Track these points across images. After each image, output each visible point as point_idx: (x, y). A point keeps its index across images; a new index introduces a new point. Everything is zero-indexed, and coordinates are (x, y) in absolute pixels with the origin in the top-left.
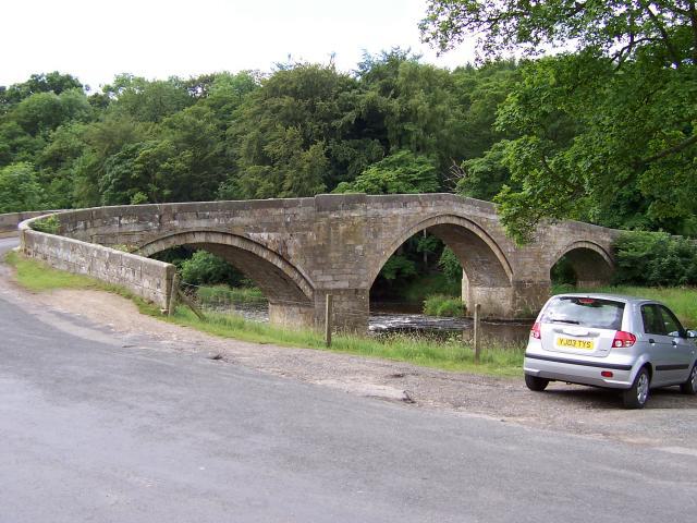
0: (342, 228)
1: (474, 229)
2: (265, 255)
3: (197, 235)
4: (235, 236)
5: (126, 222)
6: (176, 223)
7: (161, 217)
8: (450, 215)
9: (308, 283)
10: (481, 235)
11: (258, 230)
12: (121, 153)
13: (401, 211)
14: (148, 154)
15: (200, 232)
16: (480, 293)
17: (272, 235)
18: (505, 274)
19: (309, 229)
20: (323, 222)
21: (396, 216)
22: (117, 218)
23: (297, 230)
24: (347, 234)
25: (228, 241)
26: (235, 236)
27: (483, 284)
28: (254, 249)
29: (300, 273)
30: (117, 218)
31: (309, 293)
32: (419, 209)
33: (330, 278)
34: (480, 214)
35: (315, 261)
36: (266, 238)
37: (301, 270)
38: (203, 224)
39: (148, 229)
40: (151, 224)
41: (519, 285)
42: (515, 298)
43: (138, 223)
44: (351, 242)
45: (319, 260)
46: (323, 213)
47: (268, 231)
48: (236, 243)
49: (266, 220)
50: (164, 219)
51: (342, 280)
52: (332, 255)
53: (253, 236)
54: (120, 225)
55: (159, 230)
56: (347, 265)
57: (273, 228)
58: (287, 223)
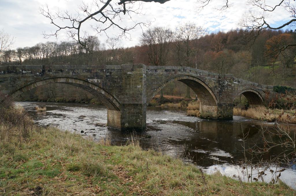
1: (200, 82)
4: (81, 80)
5: (25, 72)
9: (117, 101)
10: (203, 84)
18: (214, 101)
25: (78, 82)
26: (81, 80)
27: (206, 104)
30: (21, 70)
39: (37, 75)
40: (38, 73)
42: (218, 110)
43: (31, 73)
47: (97, 78)
48: (81, 83)
53: (90, 80)
58: (107, 76)
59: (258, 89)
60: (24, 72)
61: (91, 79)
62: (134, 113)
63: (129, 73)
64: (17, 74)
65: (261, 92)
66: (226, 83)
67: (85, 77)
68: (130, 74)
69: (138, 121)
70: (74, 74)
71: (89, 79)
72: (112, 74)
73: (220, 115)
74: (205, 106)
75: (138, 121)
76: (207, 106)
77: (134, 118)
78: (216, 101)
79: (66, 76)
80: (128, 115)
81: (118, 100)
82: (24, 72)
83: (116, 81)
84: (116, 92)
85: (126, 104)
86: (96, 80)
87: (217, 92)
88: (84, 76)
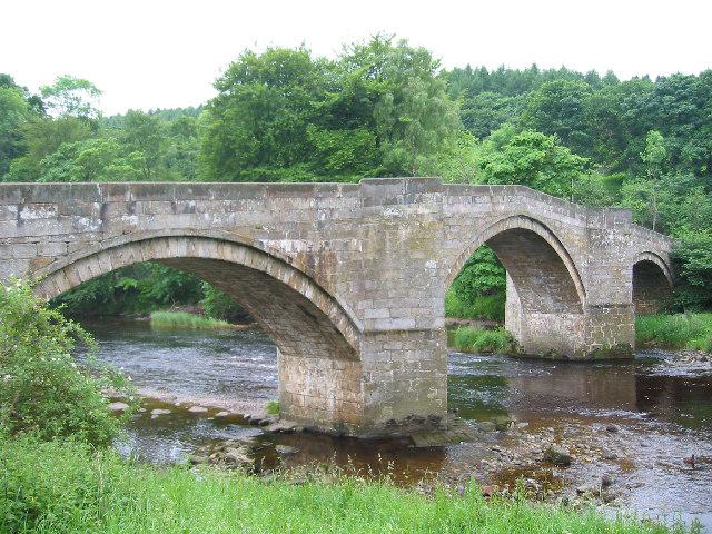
0: (404, 233)
2: (286, 277)
3: (172, 244)
5: (33, 216)
6: (134, 219)
7: (104, 207)
8: (522, 217)
9: (350, 322)
11: (277, 236)
12: (59, 154)
14: (89, 154)
15: (177, 238)
16: (537, 321)
17: (300, 246)
19: (352, 234)
20: (373, 223)
22: (13, 209)
23: (336, 235)
24: (413, 243)
25: (228, 254)
27: (544, 310)
29: (340, 307)
31: (351, 337)
33: (385, 313)
35: (362, 288)
36: (288, 249)
37: (343, 303)
38: (184, 223)
39: (78, 231)
40: (84, 221)
41: (595, 308)
44: (418, 255)
45: (368, 285)
46: (373, 208)
47: (294, 236)
48: (240, 257)
49: (291, 217)
50: (112, 212)
51: (405, 317)
52: (388, 275)
53: (268, 244)
54: (20, 222)
55: (101, 232)
56: (412, 292)
57: (300, 232)
58: (321, 225)
62: (415, 365)
68: (396, 217)
70: (215, 221)
72: (336, 215)
74: (536, 315)
76: (547, 315)
78: (582, 298)
80: (392, 372)
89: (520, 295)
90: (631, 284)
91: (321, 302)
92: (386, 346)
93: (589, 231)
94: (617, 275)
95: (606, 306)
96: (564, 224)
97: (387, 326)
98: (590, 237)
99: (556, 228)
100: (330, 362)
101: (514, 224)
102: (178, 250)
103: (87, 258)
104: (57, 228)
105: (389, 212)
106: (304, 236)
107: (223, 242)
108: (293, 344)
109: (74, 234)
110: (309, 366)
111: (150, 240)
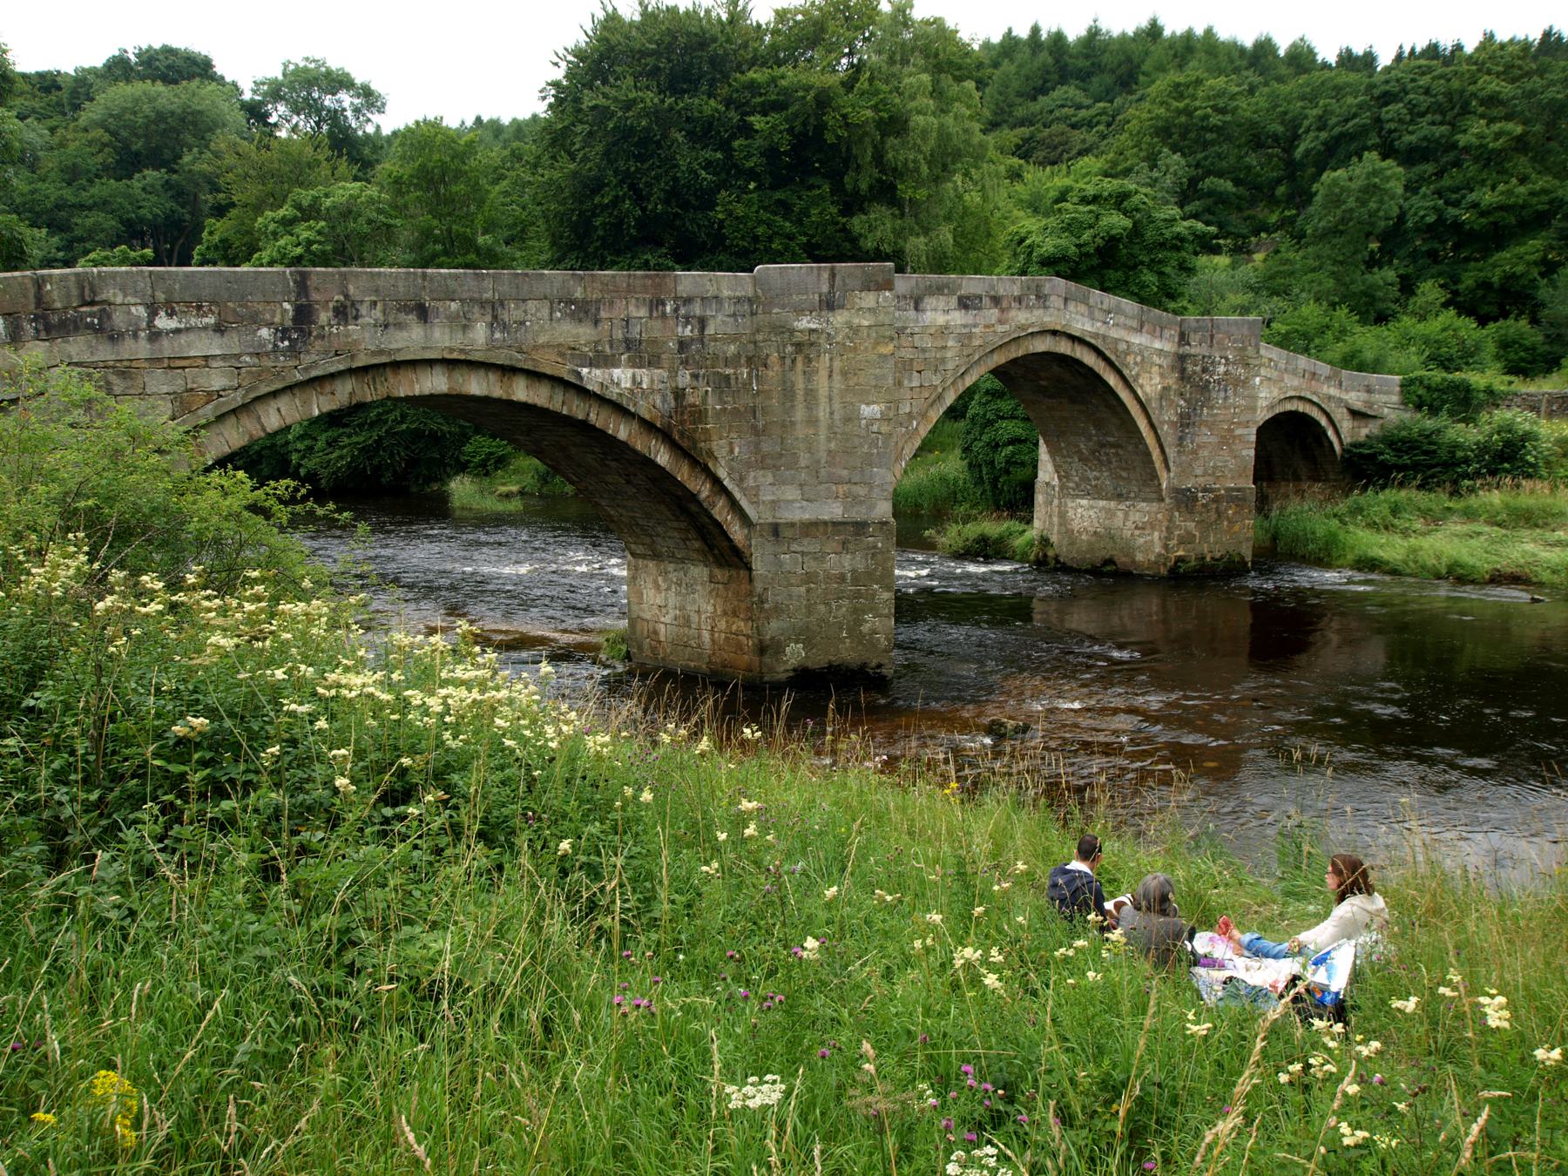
5: (173, 324)
8: (1054, 333)
9: (734, 505)
10: (1112, 380)
13: (958, 318)
15: (430, 363)
17: (645, 376)
21: (944, 331)
25: (521, 391)
27: (1097, 493)
28: (596, 417)
30: (141, 311)
31: (737, 533)
32: (993, 314)
33: (791, 493)
34: (1115, 333)
38: (441, 339)
41: (1185, 500)
43: (219, 329)
47: (636, 363)
53: (593, 377)
57: (639, 352)
58: (683, 345)
59: (1330, 398)
60: (163, 322)
61: (598, 367)
62: (842, 578)
63: (805, 323)
64: (111, 338)
65: (1341, 415)
66: (1222, 369)
67: (562, 355)
69: (865, 628)
71: (585, 371)
72: (710, 330)
73: (1181, 553)
74: (1084, 502)
75: (865, 628)
76: (1102, 503)
77: (840, 607)
79: (451, 350)
80: (803, 589)
81: (744, 503)
82: (163, 322)
83: (727, 377)
84: (732, 451)
85: (792, 525)
86: (622, 376)
87: (1172, 423)
88: (559, 345)
89: (1057, 468)
90: (1252, 453)
91: (683, 473)
92: (795, 547)
93: (1182, 358)
94: (1228, 439)
95: (1205, 490)
96: (1130, 340)
97: (800, 513)
98: (1183, 371)
99: (1116, 351)
100: (706, 571)
101: (1042, 345)
102: (435, 383)
103: (274, 394)
104: (213, 346)
105: (805, 323)
106: (654, 362)
107: (508, 371)
108: (648, 540)
109: (250, 354)
110: (673, 576)
111: (384, 365)
